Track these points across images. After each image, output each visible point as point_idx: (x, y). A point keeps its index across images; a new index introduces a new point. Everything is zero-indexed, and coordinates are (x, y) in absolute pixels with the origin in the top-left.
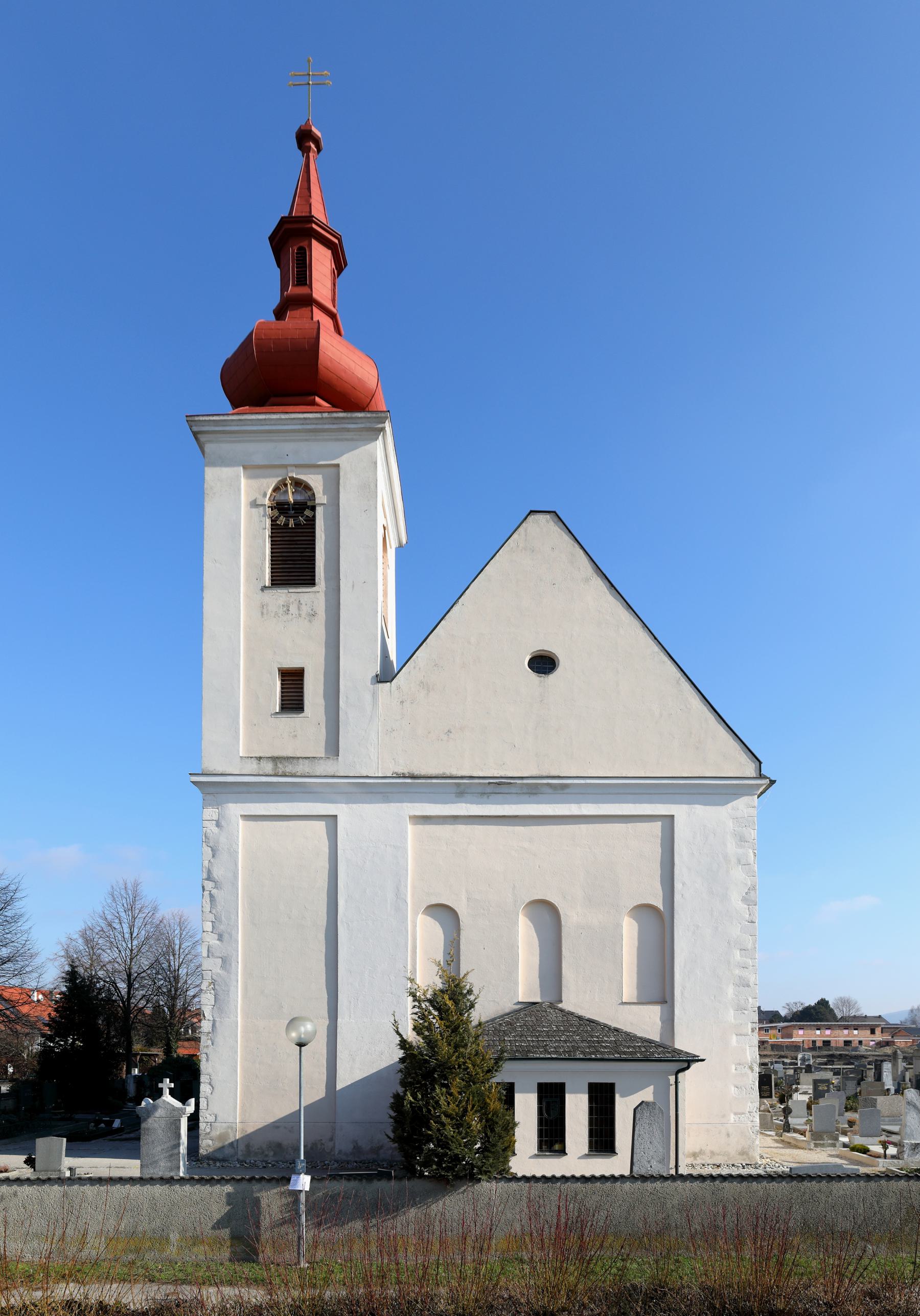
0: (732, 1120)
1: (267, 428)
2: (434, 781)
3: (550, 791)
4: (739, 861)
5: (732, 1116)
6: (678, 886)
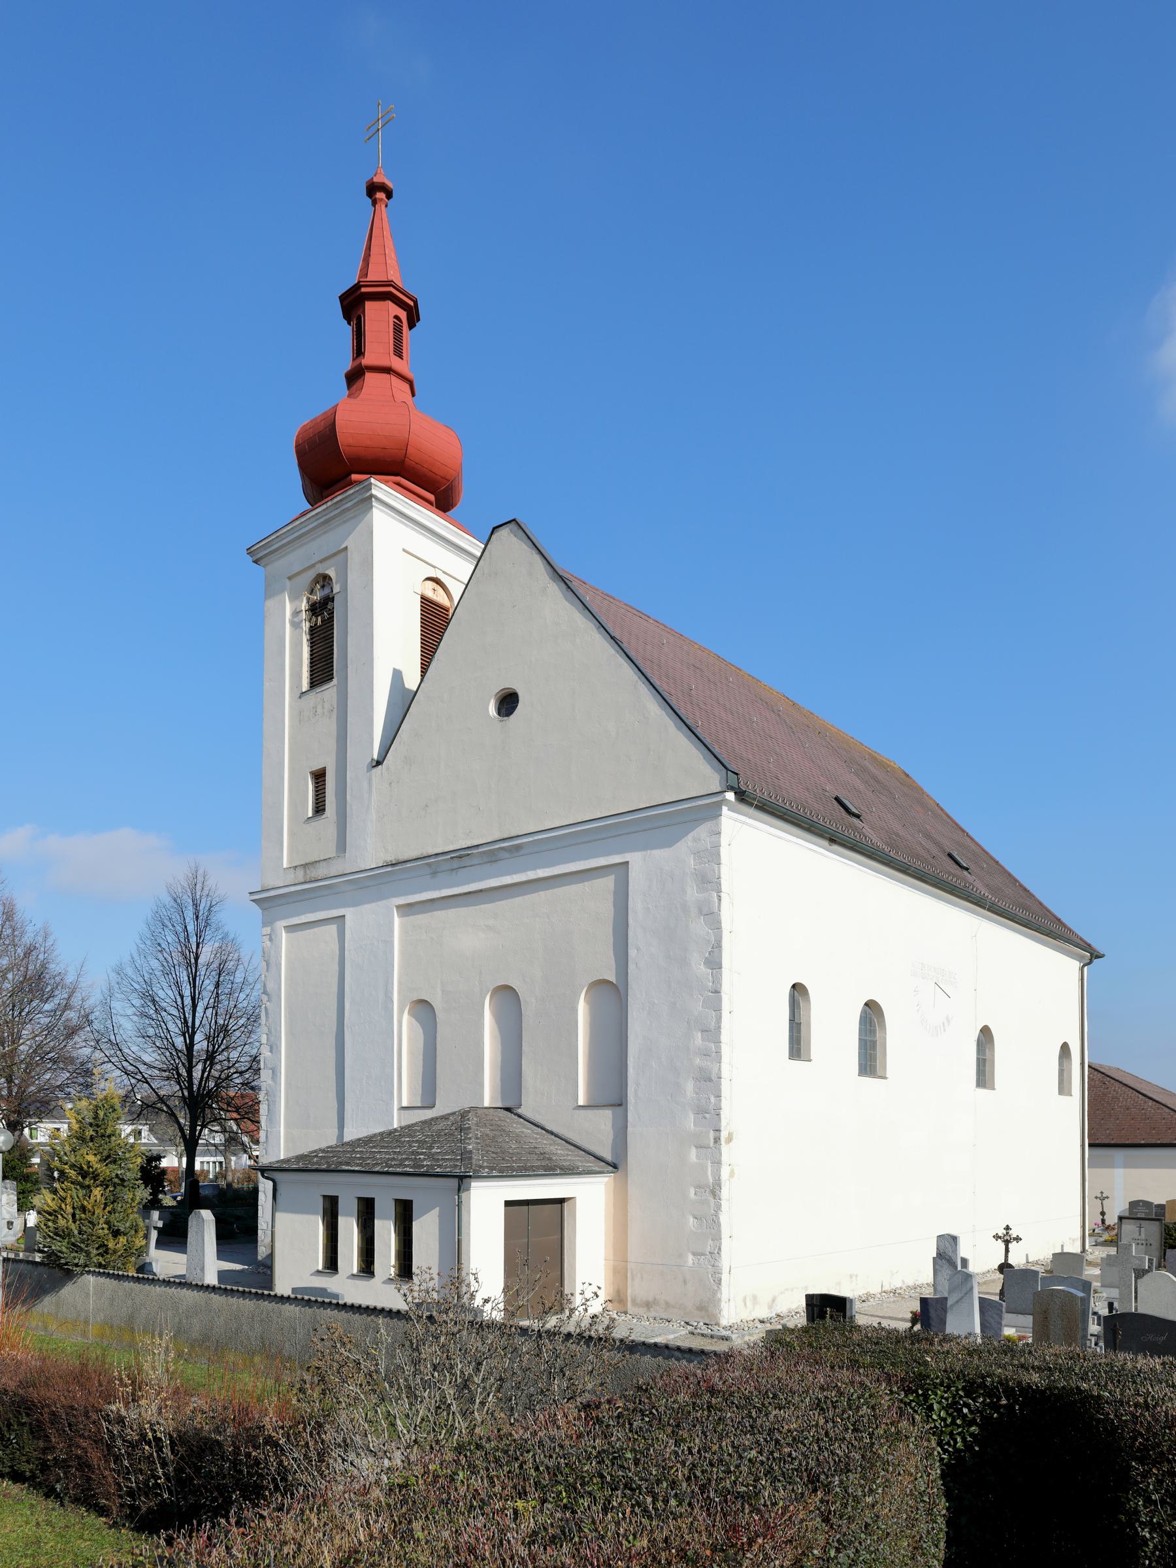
0: (690, 1262)
1: (296, 535)
2: (700, 802)
3: (506, 855)
4: (700, 911)
5: (690, 1257)
6: (632, 952)
